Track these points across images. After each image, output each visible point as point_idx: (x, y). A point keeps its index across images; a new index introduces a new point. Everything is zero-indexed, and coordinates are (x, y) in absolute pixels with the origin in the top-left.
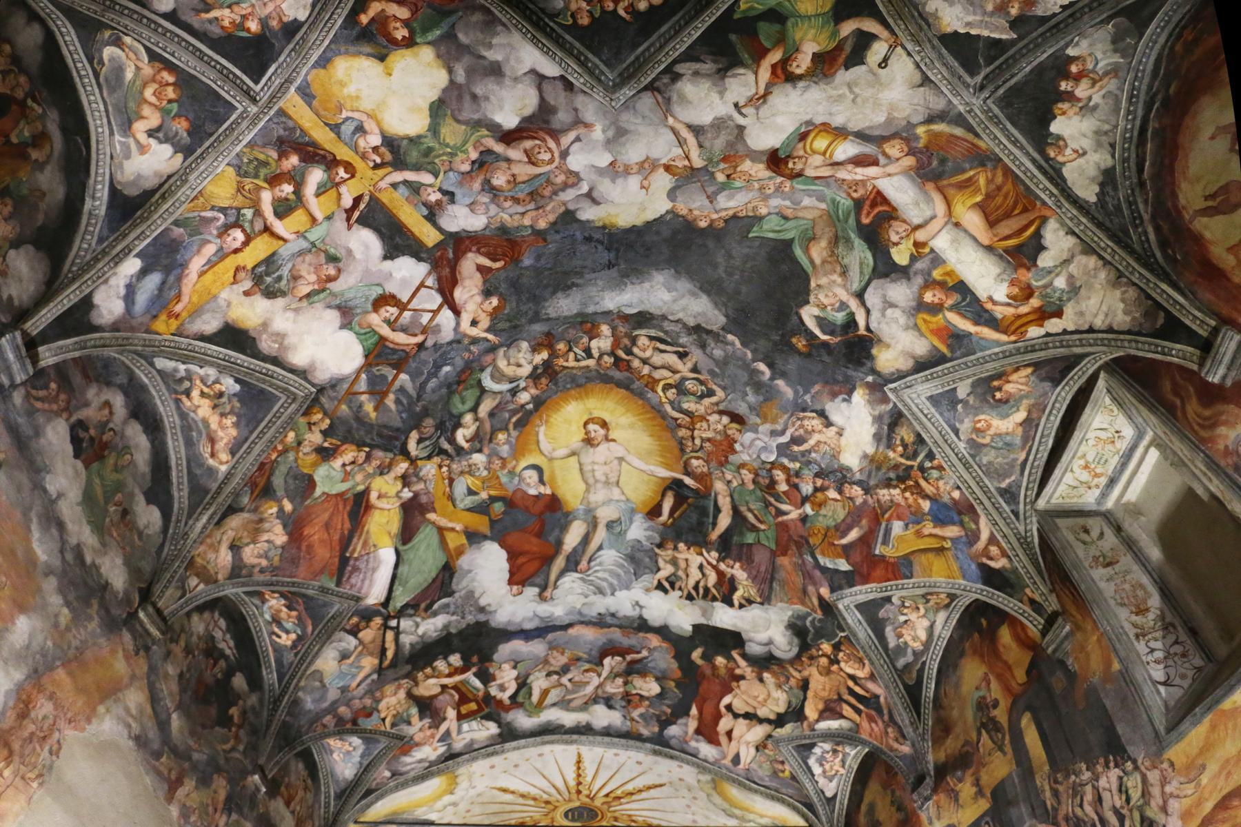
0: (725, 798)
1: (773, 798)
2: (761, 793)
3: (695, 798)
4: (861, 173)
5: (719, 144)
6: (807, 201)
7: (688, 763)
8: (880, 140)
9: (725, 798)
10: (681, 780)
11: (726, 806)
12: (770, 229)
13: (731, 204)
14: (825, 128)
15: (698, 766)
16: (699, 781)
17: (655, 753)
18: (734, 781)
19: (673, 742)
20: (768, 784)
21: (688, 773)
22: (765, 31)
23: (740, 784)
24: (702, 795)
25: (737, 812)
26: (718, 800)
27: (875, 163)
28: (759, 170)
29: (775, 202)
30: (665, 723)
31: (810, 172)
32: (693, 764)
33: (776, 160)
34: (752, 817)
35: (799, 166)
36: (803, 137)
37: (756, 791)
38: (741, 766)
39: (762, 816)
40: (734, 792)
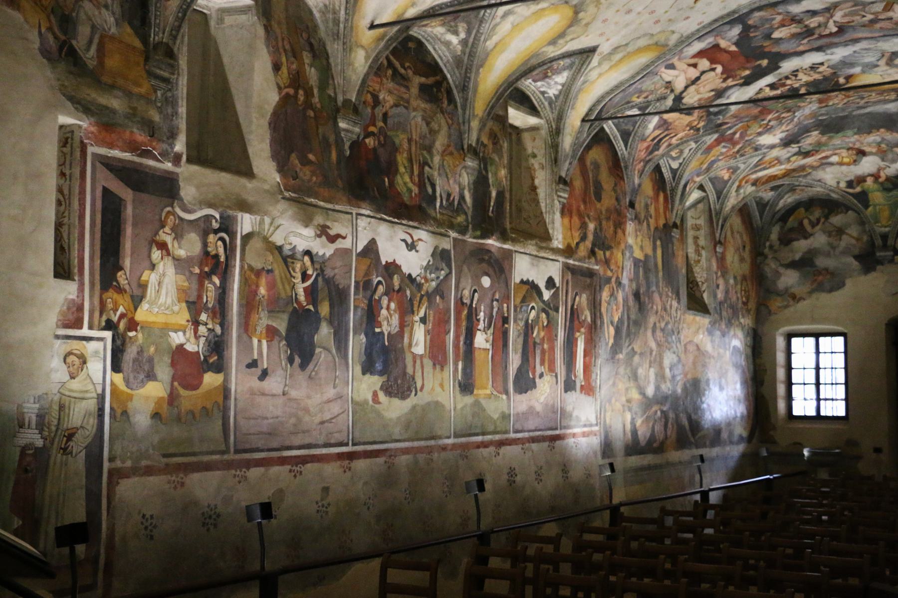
0: (640, 50)
1: (617, 87)
2: (627, 80)
3: (657, 22)
4: (823, 155)
5: (890, 156)
6: (839, 142)
7: (698, 30)
8: (822, 164)
9: (640, 50)
10: (688, 18)
11: (630, 48)
12: (849, 133)
13: (873, 138)
14: (848, 164)
15: (688, 37)
16: (673, 32)
17: (734, 12)
18: (653, 62)
19: (727, 27)
20: (634, 86)
21: (690, 26)
22: (889, 185)
23: (648, 66)
24: (657, 29)
25: (618, 56)
26: (642, 43)
27: (820, 159)
28: (867, 149)
29: (852, 140)
30: (747, 29)
31: (845, 151)
32: (693, 34)
33: (862, 153)
34: (606, 66)
35: (850, 152)
36: (855, 161)
37: (633, 77)
38: (663, 69)
39: (600, 75)
40: (643, 59)
